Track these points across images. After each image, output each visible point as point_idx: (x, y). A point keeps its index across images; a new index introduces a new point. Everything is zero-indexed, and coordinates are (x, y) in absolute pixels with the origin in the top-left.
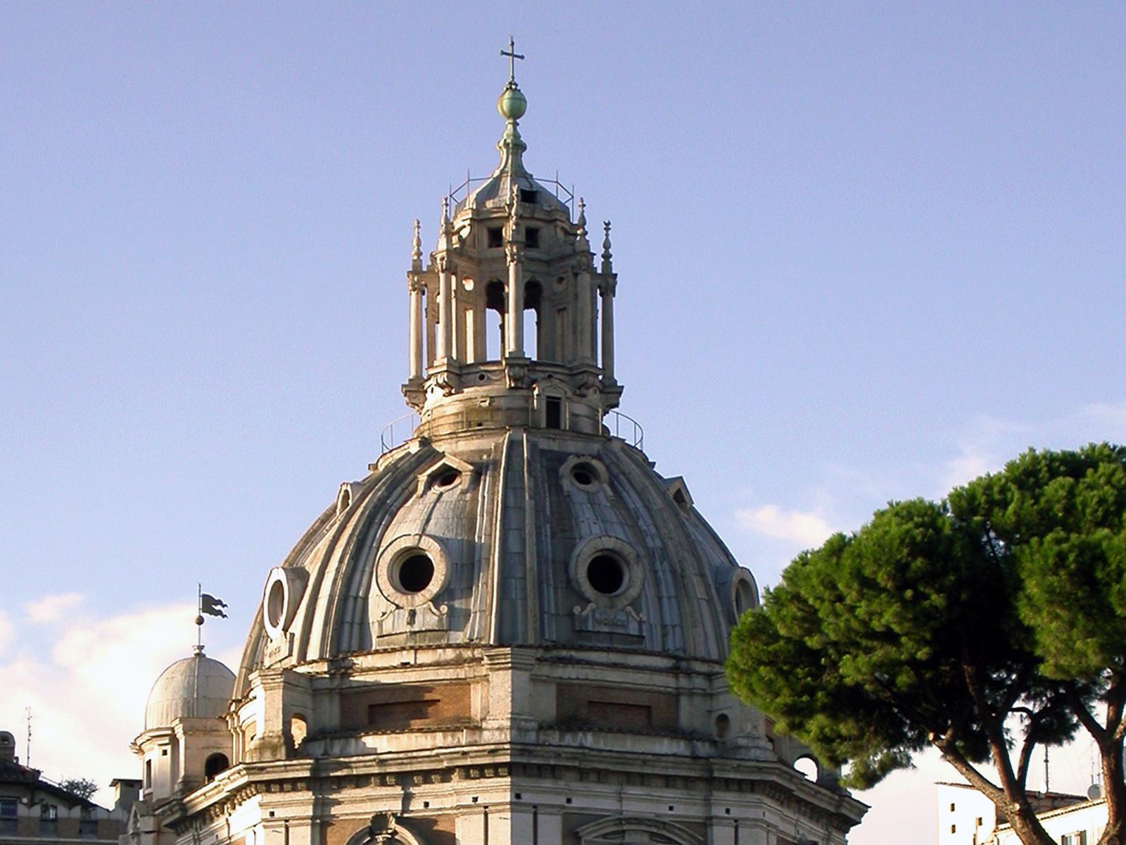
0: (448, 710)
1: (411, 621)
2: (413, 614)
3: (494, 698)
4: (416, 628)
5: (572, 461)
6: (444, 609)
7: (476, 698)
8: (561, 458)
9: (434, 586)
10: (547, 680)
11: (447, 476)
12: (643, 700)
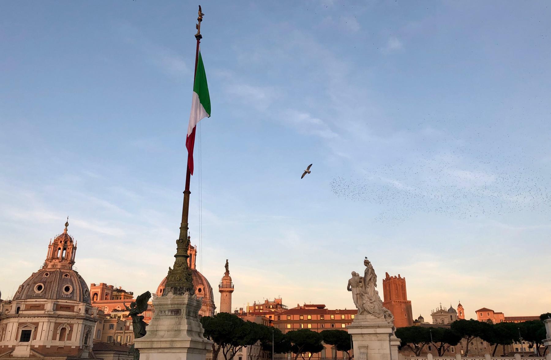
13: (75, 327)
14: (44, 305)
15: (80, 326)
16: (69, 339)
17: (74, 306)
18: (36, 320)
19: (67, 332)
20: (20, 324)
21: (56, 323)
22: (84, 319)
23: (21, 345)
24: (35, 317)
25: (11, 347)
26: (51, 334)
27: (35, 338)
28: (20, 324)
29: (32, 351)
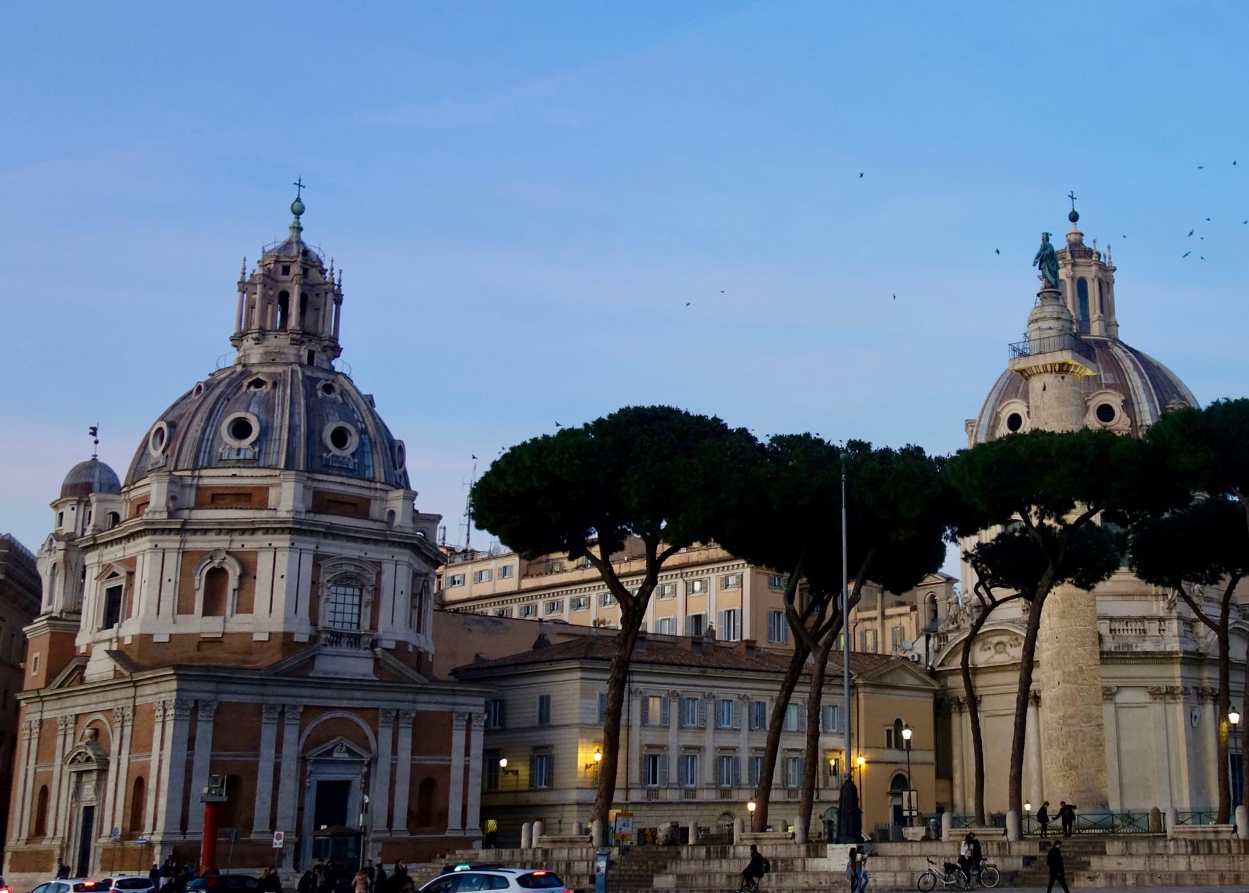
0: (256, 499)
1: (238, 454)
3: (286, 497)
5: (322, 383)
6: (257, 449)
7: (273, 494)
8: (317, 380)
9: (253, 437)
10: (309, 488)
11: (258, 383)
12: (354, 501)
13: (264, 565)
15: (283, 559)
16: (245, 607)
17: (265, 489)
19: (232, 583)
21: (185, 553)
22: (291, 531)
26: (169, 591)
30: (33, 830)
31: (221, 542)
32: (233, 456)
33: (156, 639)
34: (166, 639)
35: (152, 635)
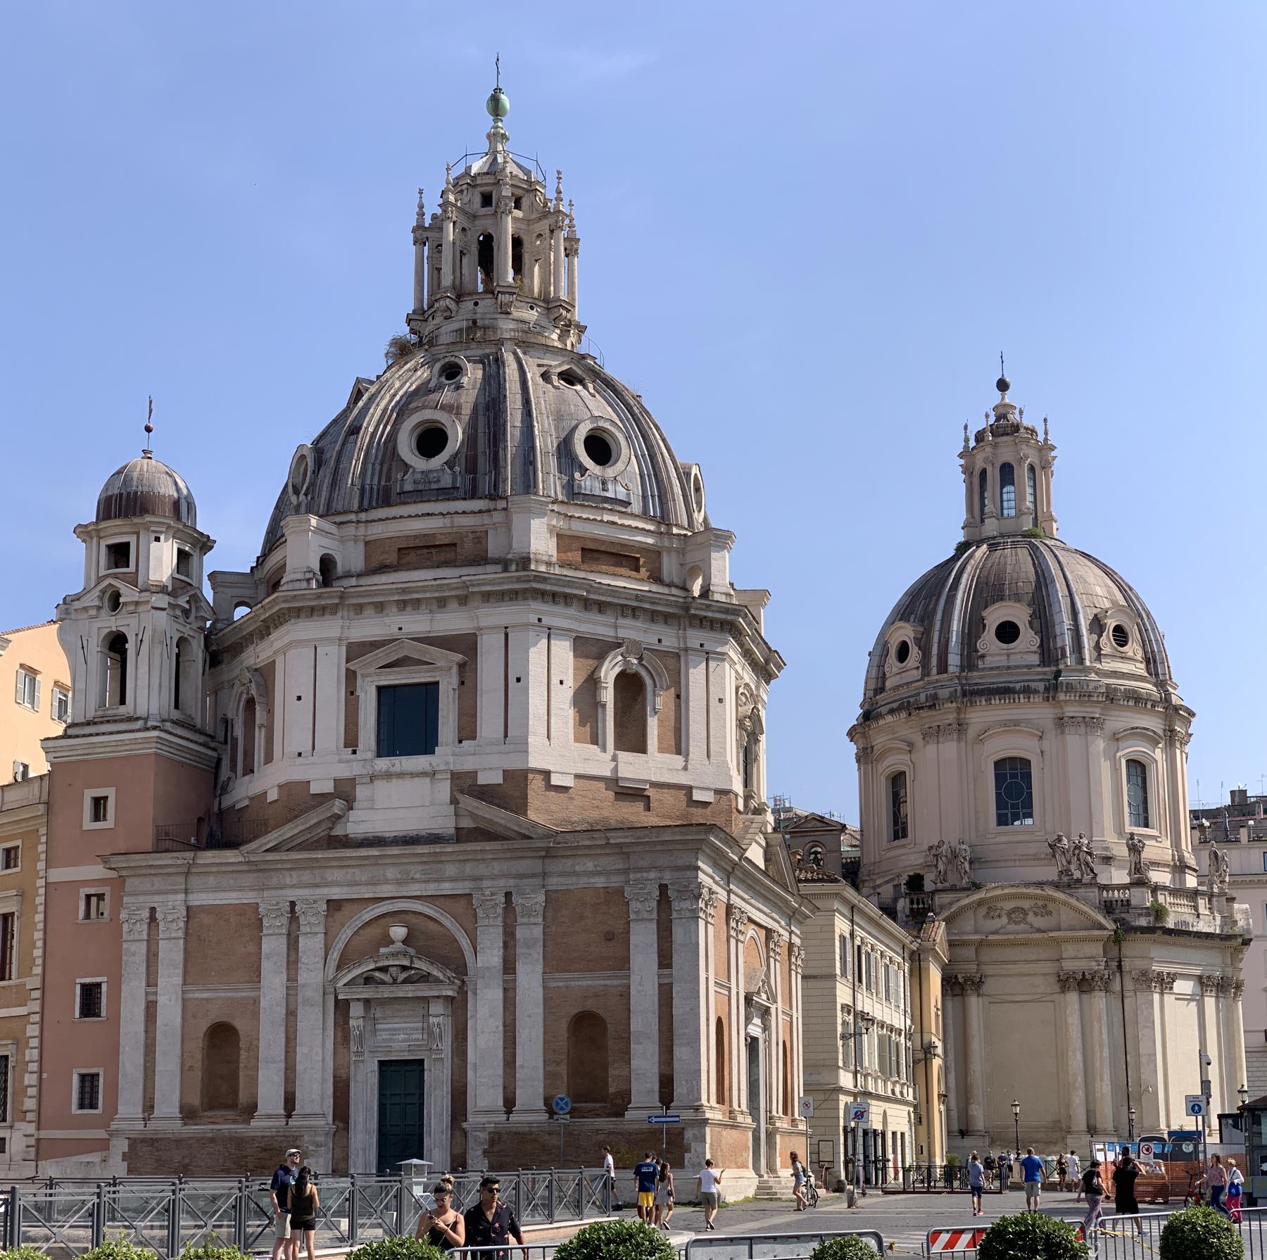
2: (604, 483)
4: (610, 494)
14: (480, 538)
18: (453, 622)
20: (356, 651)
23: (388, 776)
24: (442, 603)
25: (328, 787)
27: (467, 731)
28: (356, 651)
29: (468, 802)
30: (195, 1100)
31: (632, 630)
32: (597, 492)
33: (555, 780)
34: (568, 782)
35: (547, 774)
